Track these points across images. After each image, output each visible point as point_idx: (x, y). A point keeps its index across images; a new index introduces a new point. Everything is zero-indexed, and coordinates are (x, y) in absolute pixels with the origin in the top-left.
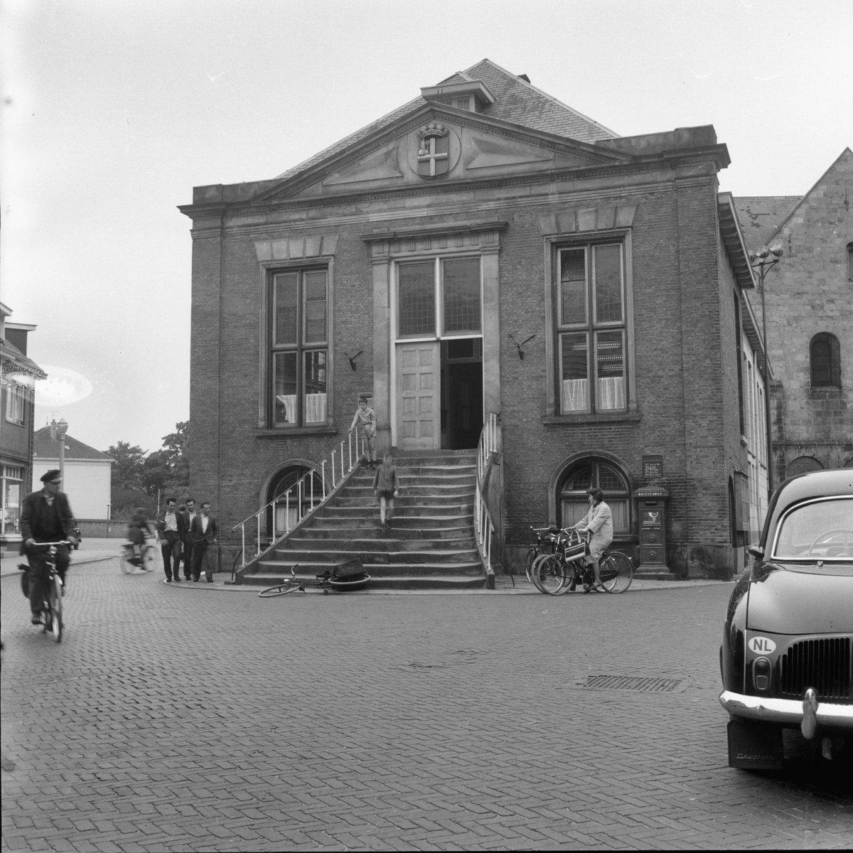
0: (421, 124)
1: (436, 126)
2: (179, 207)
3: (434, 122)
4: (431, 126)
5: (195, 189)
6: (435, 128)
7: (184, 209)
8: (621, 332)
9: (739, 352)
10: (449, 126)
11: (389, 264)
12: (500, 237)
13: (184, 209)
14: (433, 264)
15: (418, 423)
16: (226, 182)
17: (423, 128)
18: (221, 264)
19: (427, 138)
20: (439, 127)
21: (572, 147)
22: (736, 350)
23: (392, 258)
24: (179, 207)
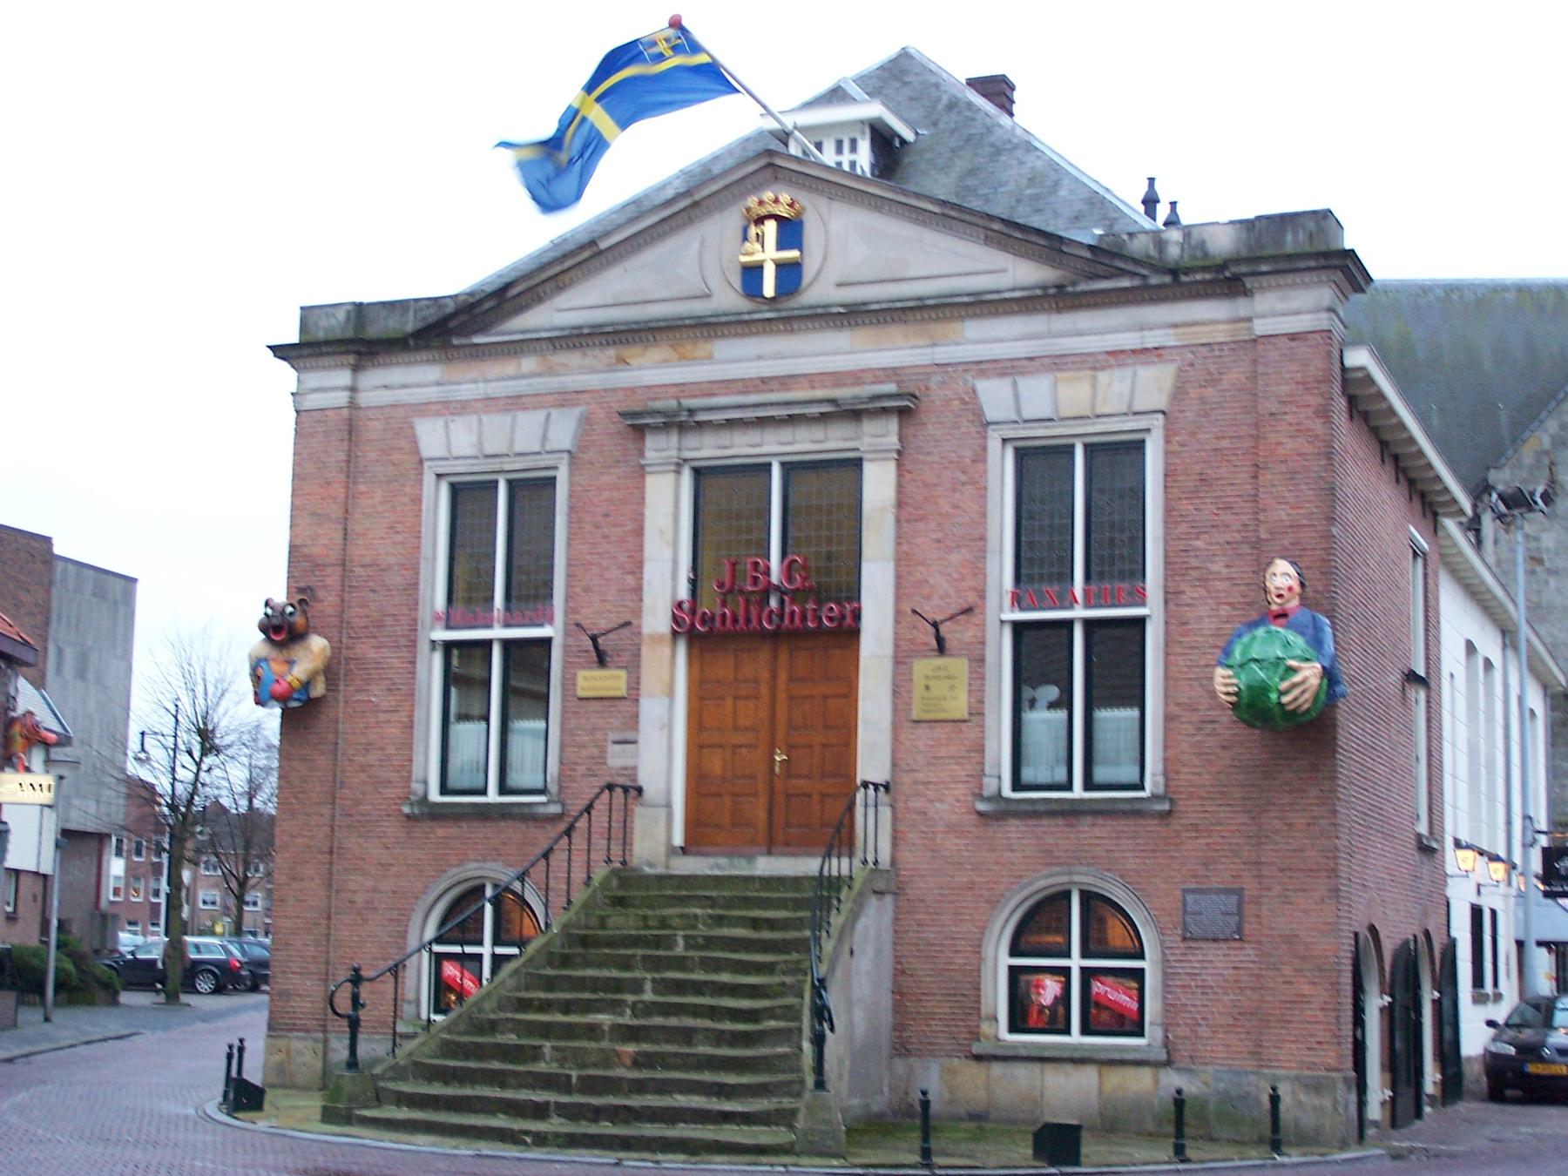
0: (750, 192)
1: (779, 198)
2: (269, 347)
3: (777, 186)
4: (768, 195)
5: (302, 308)
6: (776, 201)
7: (280, 351)
8: (496, 482)
9: (546, 906)
10: (805, 199)
11: (678, 472)
12: (901, 426)
13: (280, 351)
14: (769, 471)
15: (727, 800)
16: (366, 299)
17: (752, 201)
18: (348, 462)
19: (760, 221)
20: (785, 198)
21: (1048, 245)
22: (349, 995)
23: (685, 460)
24: (269, 347)
